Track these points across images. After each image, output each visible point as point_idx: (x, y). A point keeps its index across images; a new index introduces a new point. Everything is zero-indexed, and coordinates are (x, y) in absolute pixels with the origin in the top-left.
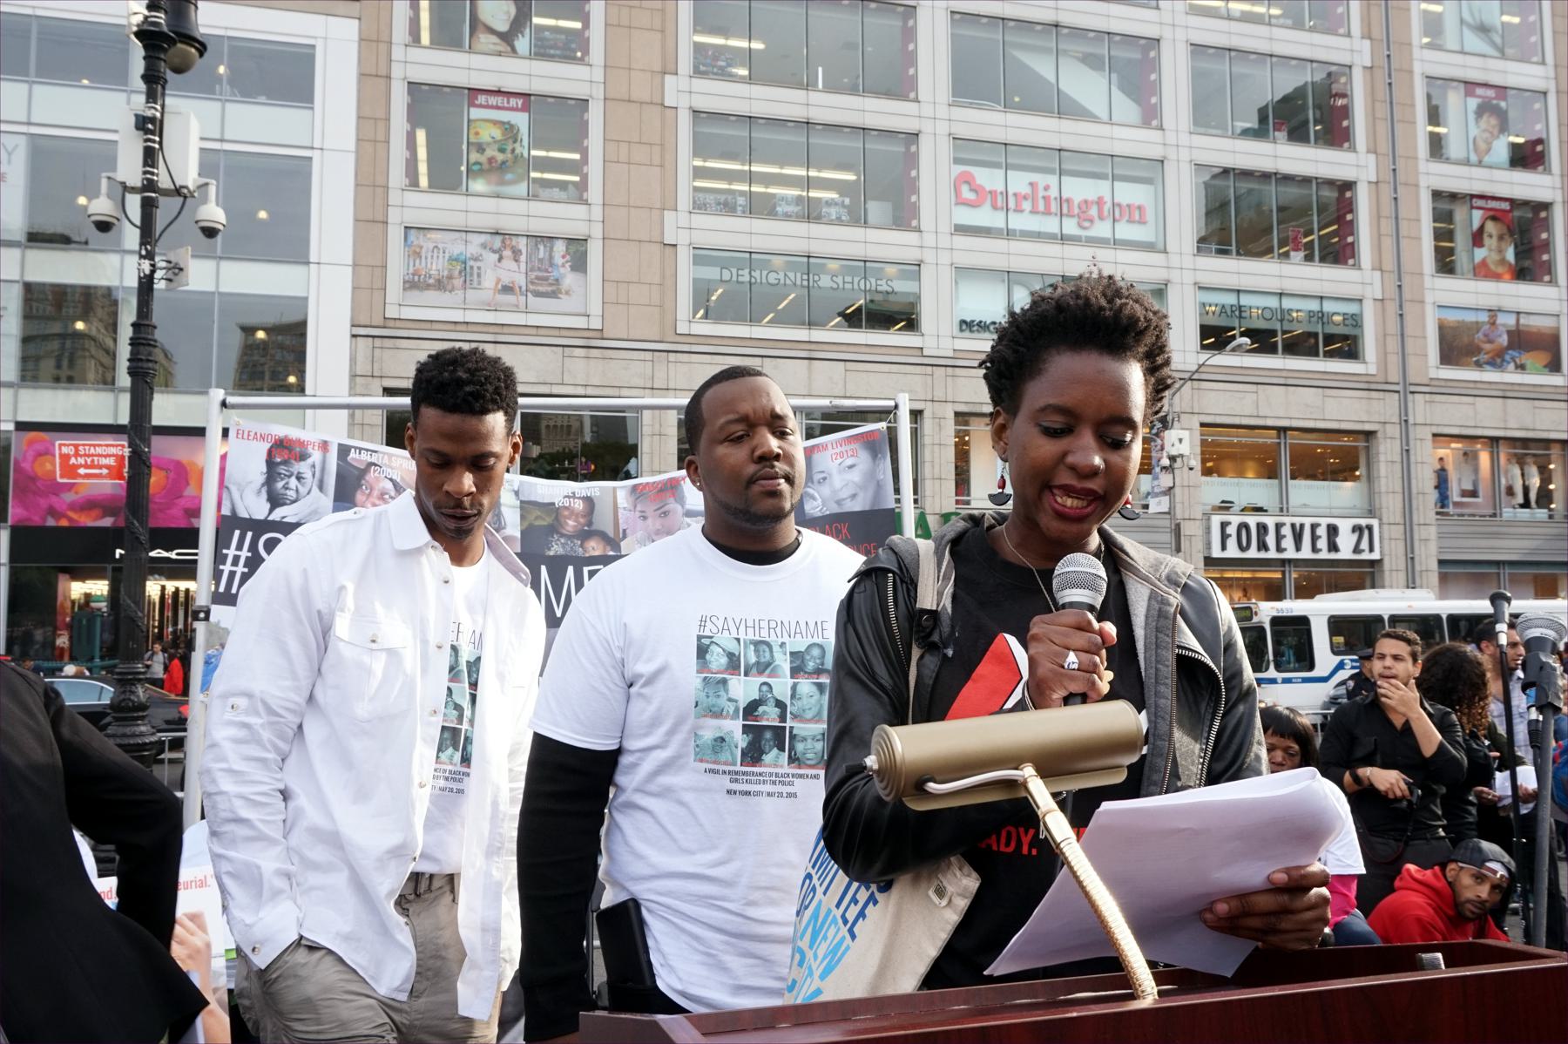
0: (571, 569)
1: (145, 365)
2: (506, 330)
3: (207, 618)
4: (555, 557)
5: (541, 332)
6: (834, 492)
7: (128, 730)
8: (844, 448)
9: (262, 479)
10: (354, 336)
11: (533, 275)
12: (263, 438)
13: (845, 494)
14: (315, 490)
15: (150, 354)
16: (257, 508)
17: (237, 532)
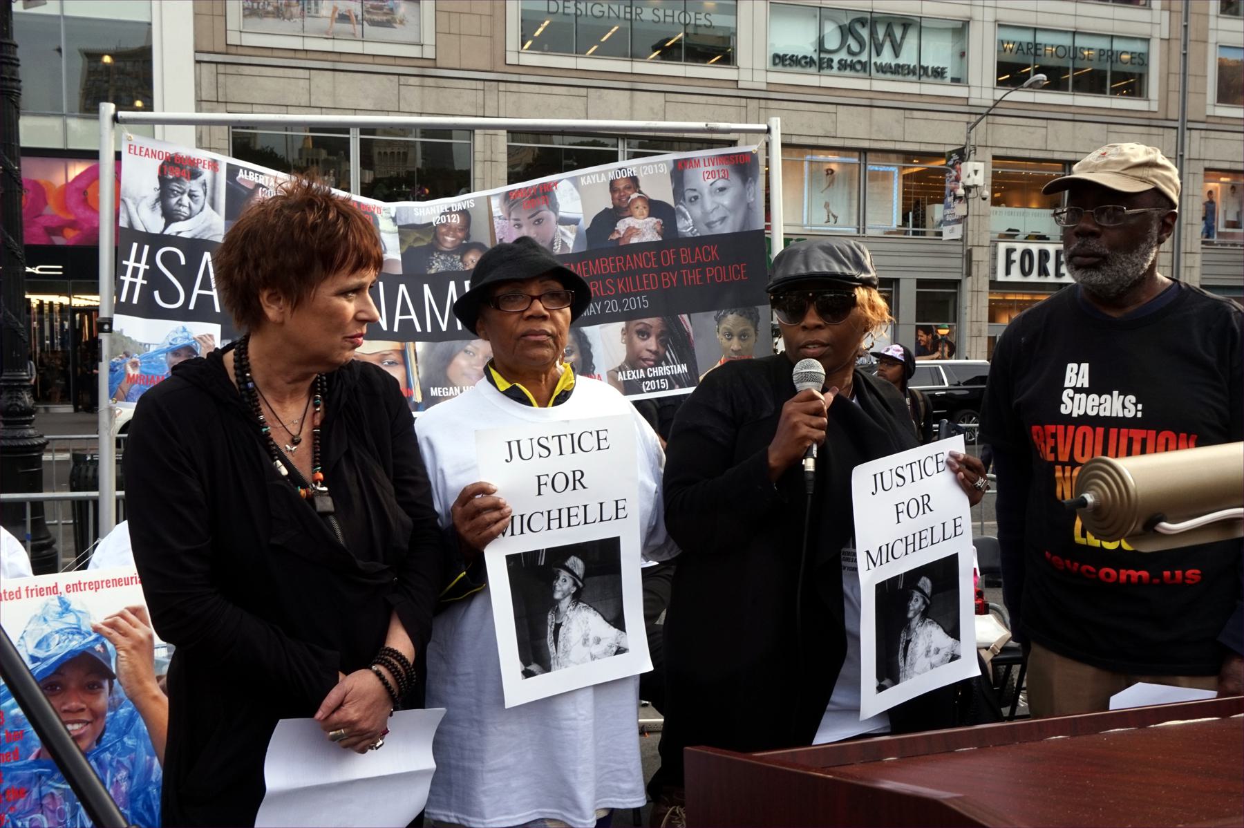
0: (452, 285)
1: (9, 84)
2: (343, 58)
3: (110, 330)
4: (438, 275)
5: (377, 60)
6: (706, 214)
7: (18, 433)
8: (716, 168)
9: (155, 194)
10: (198, 62)
12: (154, 154)
14: (207, 207)
15: (14, 73)
16: (151, 221)
17: (135, 245)
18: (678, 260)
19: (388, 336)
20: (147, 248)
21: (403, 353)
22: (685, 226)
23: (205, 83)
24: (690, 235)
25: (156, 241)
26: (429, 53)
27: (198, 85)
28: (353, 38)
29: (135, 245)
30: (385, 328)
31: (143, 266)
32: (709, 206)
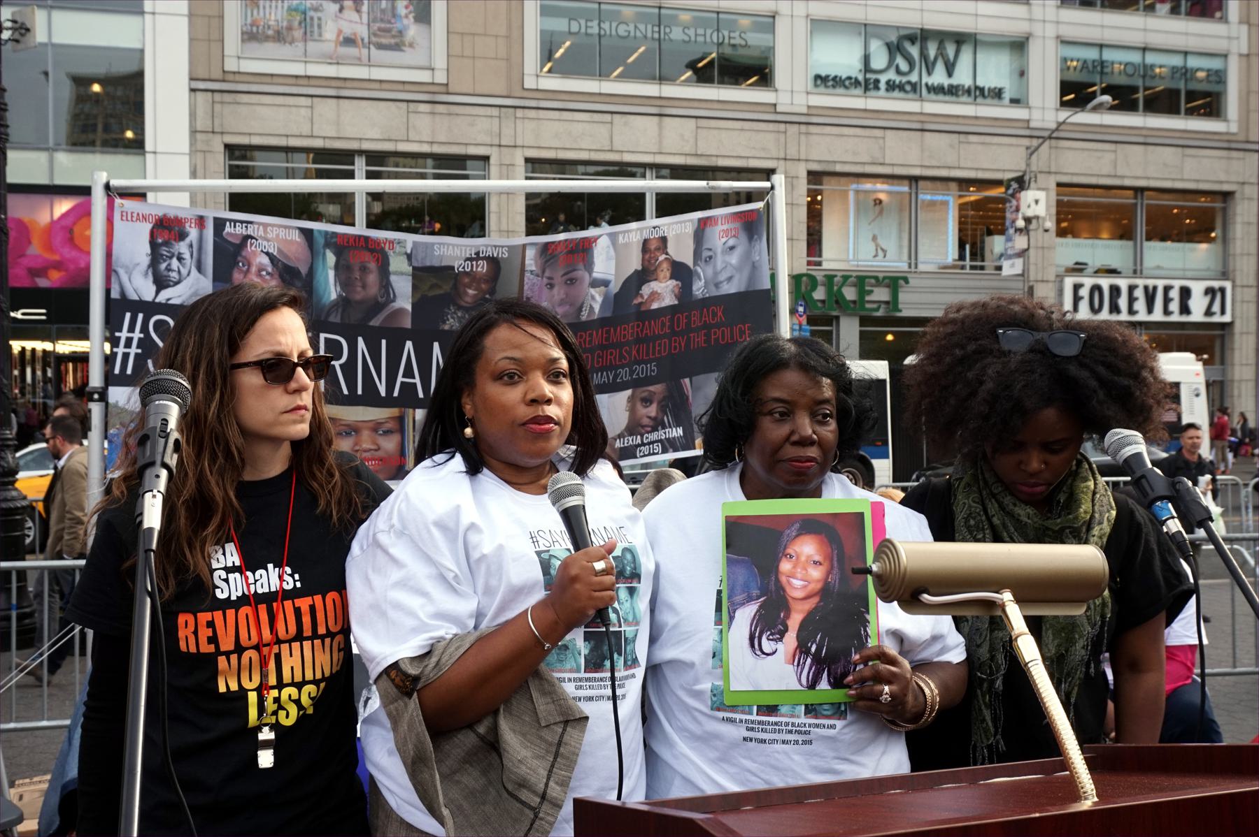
2: (348, 84)
5: (385, 86)
11: (375, 26)
13: (723, 277)
16: (144, 289)
17: (128, 315)
18: (688, 324)
19: (387, 402)
20: (141, 316)
21: (401, 420)
22: (699, 289)
23: (200, 113)
24: (701, 296)
25: (150, 308)
26: (441, 78)
27: (193, 115)
28: (358, 62)
29: (128, 315)
30: (383, 394)
31: (137, 335)
32: (719, 265)
